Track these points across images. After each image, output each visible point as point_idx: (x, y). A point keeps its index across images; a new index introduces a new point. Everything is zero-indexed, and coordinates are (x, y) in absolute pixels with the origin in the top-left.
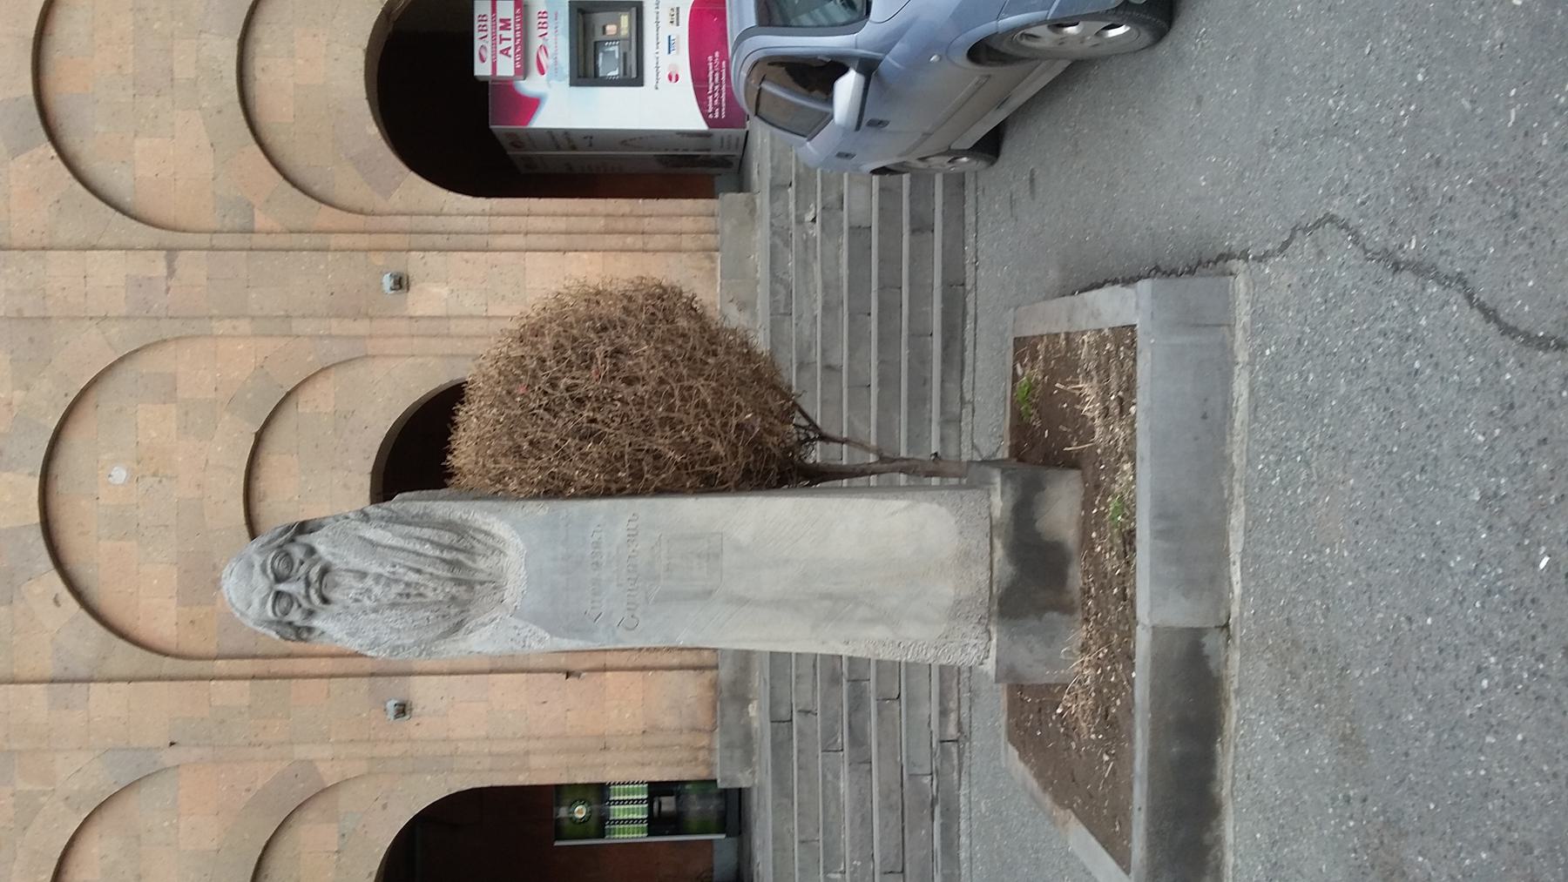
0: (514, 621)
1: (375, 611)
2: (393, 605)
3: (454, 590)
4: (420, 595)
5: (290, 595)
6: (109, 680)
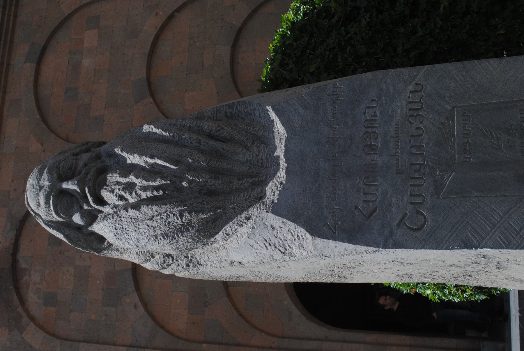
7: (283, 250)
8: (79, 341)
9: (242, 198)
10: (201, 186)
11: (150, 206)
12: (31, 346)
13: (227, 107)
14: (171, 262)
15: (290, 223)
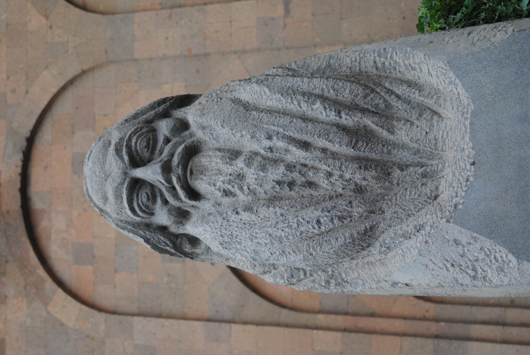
0: (454, 231)
1: (248, 208)
2: (273, 200)
3: (358, 177)
4: (310, 184)
5: (152, 186)
6: (245, 323)
7: (472, 273)
8: (133, 315)
9: (408, 197)
10: (346, 181)
11: (271, 209)
12: (62, 324)
13: (376, 55)
14: (302, 276)
15: (483, 238)
